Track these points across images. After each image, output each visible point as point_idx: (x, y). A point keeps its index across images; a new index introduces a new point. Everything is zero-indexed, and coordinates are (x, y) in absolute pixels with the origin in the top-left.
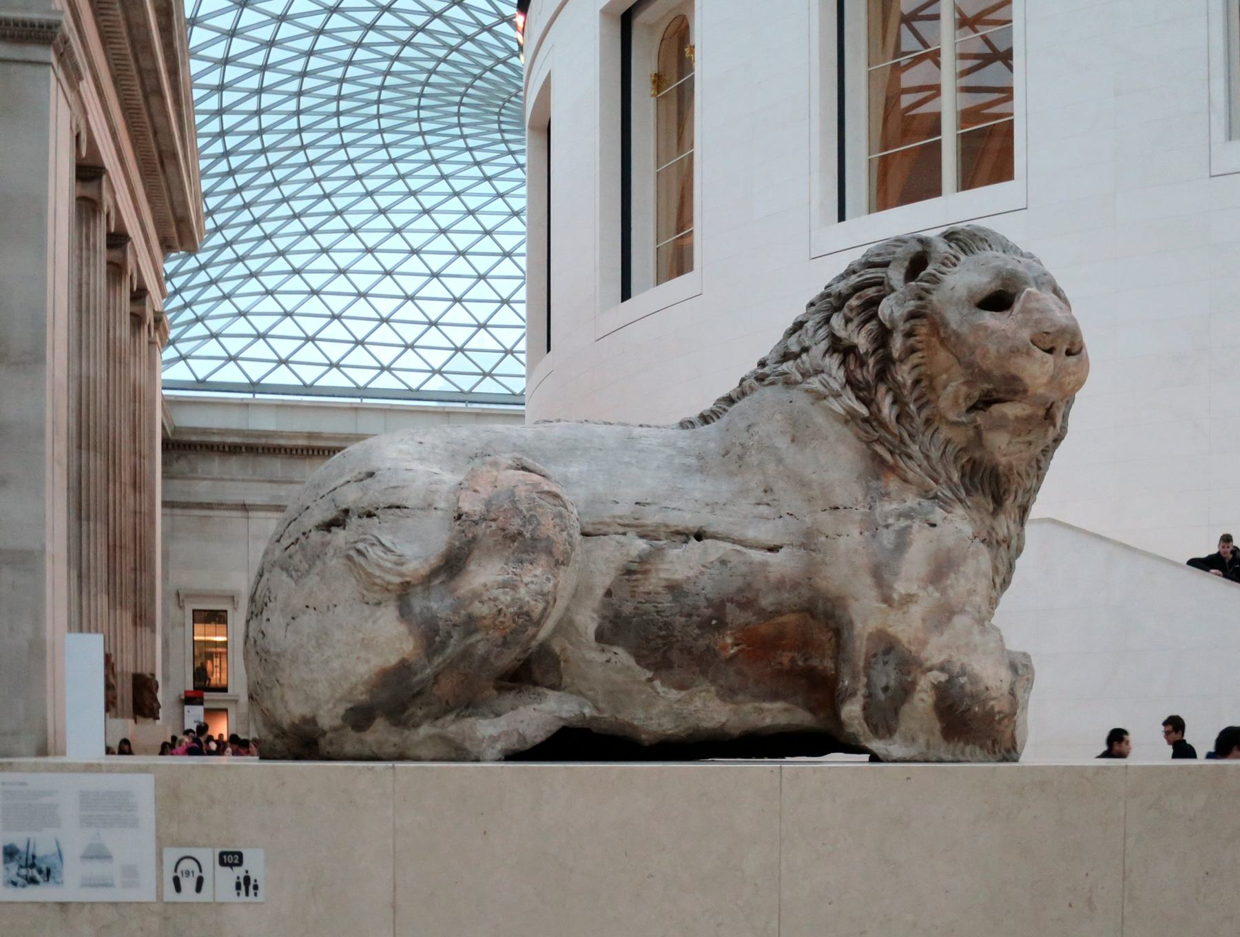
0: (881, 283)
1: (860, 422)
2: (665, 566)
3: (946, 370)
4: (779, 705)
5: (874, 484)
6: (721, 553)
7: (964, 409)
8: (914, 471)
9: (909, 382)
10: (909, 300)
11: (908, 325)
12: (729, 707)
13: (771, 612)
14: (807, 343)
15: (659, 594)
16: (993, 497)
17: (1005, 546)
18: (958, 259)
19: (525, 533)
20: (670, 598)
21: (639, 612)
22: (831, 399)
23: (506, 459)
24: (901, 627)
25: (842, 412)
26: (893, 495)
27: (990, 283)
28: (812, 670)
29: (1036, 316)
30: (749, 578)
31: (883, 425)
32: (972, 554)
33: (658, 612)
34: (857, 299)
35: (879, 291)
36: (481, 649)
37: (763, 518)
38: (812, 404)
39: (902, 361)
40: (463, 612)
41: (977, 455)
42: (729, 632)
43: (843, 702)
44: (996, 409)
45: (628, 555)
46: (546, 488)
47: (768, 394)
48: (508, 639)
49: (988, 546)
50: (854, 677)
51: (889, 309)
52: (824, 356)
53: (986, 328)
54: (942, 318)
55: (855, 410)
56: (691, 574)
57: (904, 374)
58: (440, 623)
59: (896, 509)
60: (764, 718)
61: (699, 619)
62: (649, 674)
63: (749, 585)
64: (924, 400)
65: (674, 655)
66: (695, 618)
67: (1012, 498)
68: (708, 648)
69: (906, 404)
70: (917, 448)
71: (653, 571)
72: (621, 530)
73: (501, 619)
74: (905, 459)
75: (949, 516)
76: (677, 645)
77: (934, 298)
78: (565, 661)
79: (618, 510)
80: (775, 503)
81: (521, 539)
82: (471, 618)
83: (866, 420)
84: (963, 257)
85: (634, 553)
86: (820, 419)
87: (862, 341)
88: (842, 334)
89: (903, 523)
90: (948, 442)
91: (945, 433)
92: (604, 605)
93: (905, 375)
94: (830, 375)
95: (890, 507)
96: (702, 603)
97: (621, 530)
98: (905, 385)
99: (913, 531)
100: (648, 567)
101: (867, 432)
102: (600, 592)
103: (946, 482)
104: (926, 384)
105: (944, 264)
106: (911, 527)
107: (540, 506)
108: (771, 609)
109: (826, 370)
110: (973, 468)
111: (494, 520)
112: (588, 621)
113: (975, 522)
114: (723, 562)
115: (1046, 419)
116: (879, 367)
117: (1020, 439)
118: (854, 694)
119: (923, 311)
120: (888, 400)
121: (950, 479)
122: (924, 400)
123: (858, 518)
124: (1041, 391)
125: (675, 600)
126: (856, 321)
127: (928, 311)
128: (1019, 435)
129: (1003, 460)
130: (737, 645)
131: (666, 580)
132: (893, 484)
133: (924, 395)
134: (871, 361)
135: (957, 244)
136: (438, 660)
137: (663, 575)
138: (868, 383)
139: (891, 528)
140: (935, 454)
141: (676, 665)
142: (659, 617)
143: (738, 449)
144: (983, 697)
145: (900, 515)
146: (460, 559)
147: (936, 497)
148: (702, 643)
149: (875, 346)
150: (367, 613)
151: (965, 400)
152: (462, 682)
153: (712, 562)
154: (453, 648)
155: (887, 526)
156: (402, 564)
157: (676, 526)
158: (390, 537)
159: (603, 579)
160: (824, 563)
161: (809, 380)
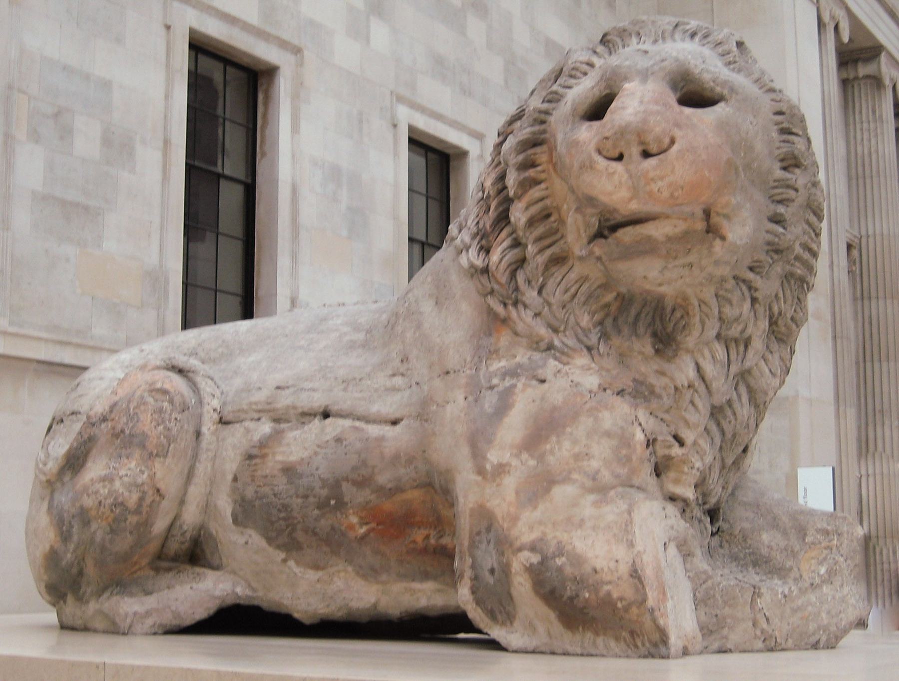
2: (281, 449)
4: (429, 586)
6: (339, 430)
10: (525, 128)
11: (521, 157)
13: (390, 489)
15: (275, 476)
16: (655, 335)
19: (126, 430)
20: (284, 480)
21: (259, 495)
27: (593, 88)
32: (588, 411)
33: (275, 495)
37: (395, 389)
39: (519, 197)
40: (77, 505)
41: (623, 290)
42: (351, 511)
44: (626, 235)
45: (251, 440)
46: (159, 385)
49: (635, 397)
56: (305, 454)
57: (519, 215)
58: (65, 515)
59: (502, 367)
61: (316, 500)
62: (283, 555)
65: (300, 536)
66: (311, 499)
68: (333, 528)
70: (535, 293)
71: (270, 455)
72: (256, 416)
75: (567, 368)
76: (299, 527)
77: (552, 119)
78: (221, 543)
80: (409, 372)
82: (82, 508)
83: (486, 270)
85: (256, 437)
86: (454, 277)
89: (508, 382)
90: (583, 279)
92: (234, 490)
95: (499, 365)
96: (317, 484)
99: (517, 390)
100: (266, 451)
102: (230, 477)
106: (514, 386)
107: (145, 404)
108: (389, 486)
112: (225, 505)
113: (608, 370)
114: (338, 440)
115: (708, 232)
116: (501, 209)
117: (677, 262)
119: (543, 136)
120: (506, 244)
121: (578, 324)
122: (558, 236)
123: (463, 381)
125: (290, 482)
127: (547, 135)
128: (676, 258)
130: (367, 524)
131: (282, 462)
132: (504, 339)
137: (279, 458)
139: (496, 389)
141: (305, 546)
142: (277, 500)
144: (591, 581)
145: (507, 373)
146: (78, 458)
147: (550, 347)
148: (324, 524)
149: (500, 186)
153: (328, 441)
155: (491, 388)
157: (302, 407)
159: (231, 463)
160: (434, 434)
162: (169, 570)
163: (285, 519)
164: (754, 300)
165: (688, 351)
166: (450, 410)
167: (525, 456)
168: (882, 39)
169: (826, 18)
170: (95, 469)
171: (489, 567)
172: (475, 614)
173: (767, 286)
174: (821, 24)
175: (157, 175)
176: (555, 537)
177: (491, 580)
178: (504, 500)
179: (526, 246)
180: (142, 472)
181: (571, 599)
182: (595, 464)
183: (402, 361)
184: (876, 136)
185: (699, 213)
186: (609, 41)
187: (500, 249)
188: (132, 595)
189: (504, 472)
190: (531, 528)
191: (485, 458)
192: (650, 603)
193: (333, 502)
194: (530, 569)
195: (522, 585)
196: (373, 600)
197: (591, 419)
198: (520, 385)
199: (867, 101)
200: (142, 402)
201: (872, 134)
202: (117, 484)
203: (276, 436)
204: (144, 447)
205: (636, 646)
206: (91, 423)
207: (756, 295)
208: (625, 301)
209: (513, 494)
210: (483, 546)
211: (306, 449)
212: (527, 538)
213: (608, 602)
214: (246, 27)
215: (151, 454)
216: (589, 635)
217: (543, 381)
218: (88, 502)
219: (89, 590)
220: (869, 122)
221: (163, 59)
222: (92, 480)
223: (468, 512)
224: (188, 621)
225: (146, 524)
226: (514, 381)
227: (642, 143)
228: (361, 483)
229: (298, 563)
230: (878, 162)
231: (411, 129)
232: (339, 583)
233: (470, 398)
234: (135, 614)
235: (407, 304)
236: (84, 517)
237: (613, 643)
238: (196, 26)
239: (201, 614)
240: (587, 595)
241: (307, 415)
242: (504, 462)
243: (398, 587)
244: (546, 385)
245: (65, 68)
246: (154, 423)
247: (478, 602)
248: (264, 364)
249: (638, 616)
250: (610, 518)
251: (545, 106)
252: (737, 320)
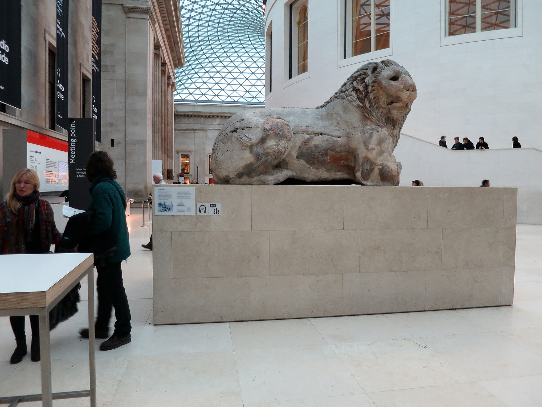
0: (366, 74)
1: (360, 107)
3: (382, 95)
5: (364, 122)
6: (327, 138)
7: (386, 105)
8: (374, 119)
9: (373, 98)
11: (372, 84)
12: (328, 174)
14: (347, 89)
17: (396, 137)
18: (385, 68)
22: (353, 102)
23: (275, 116)
24: (371, 155)
25: (356, 105)
28: (349, 165)
29: (405, 82)
30: (334, 144)
31: (366, 108)
34: (360, 78)
35: (365, 76)
36: (269, 160)
38: (349, 103)
39: (371, 93)
41: (389, 115)
43: (356, 172)
44: (394, 104)
45: (304, 139)
46: (285, 123)
47: (338, 101)
48: (276, 158)
50: (359, 167)
51: (367, 80)
52: (352, 92)
53: (392, 85)
54: (381, 82)
55: (358, 104)
57: (371, 96)
60: (336, 176)
62: (309, 166)
63: (333, 146)
64: (376, 102)
65: (315, 161)
66: (320, 153)
67: (397, 126)
68: (324, 160)
69: (372, 103)
72: (303, 133)
73: (275, 153)
74: (372, 116)
75: (382, 130)
77: (379, 77)
79: (302, 128)
81: (279, 135)
82: (267, 152)
83: (362, 107)
84: (386, 67)
85: (306, 138)
86: (351, 107)
87: (361, 88)
88: (356, 86)
89: (371, 131)
90: (382, 112)
91: (381, 110)
92: (299, 150)
93: (372, 96)
94: (353, 96)
97: (303, 133)
98: (372, 99)
100: (309, 141)
101: (362, 110)
102: (298, 147)
103: (381, 122)
104: (377, 98)
105: (381, 69)
109: (352, 95)
110: (388, 119)
111: (273, 130)
112: (295, 154)
114: (327, 140)
118: (359, 171)
120: (367, 102)
121: (383, 121)
122: (376, 102)
124: (405, 100)
125: (316, 149)
126: (360, 83)
127: (377, 81)
129: (395, 117)
132: (369, 122)
133: (376, 101)
134: (363, 93)
135: (384, 64)
136: (259, 162)
137: (313, 143)
138: (363, 98)
140: (379, 115)
143: (331, 114)
145: (370, 130)
147: (379, 125)
149: (364, 89)
150: (242, 152)
151: (386, 102)
152: (265, 167)
154: (263, 160)
155: (367, 132)
156: (251, 140)
158: (248, 135)
159: (298, 144)
160: (352, 141)
161: (348, 98)
162: (276, 169)
163: (313, 158)
165: (395, 129)
167: (378, 147)
168: (161, 46)
170: (271, 143)
171: (366, 169)
176: (385, 163)
177: (366, 171)
178: (373, 155)
180: (286, 144)
183: (337, 124)
186: (385, 63)
188: (270, 175)
190: (380, 161)
194: (380, 169)
196: (327, 176)
204: (287, 138)
208: (388, 118)
209: (375, 154)
210: (365, 164)
211: (319, 142)
212: (380, 163)
213: (393, 176)
215: (288, 140)
217: (379, 132)
218: (270, 151)
219: (254, 174)
222: (271, 145)
223: (362, 157)
226: (373, 131)
227: (413, 89)
228: (332, 150)
229: (312, 168)
232: (321, 172)
233: (362, 134)
235: (335, 111)
236: (267, 154)
240: (389, 174)
241: (318, 134)
242: (373, 147)
243: (333, 173)
246: (288, 132)
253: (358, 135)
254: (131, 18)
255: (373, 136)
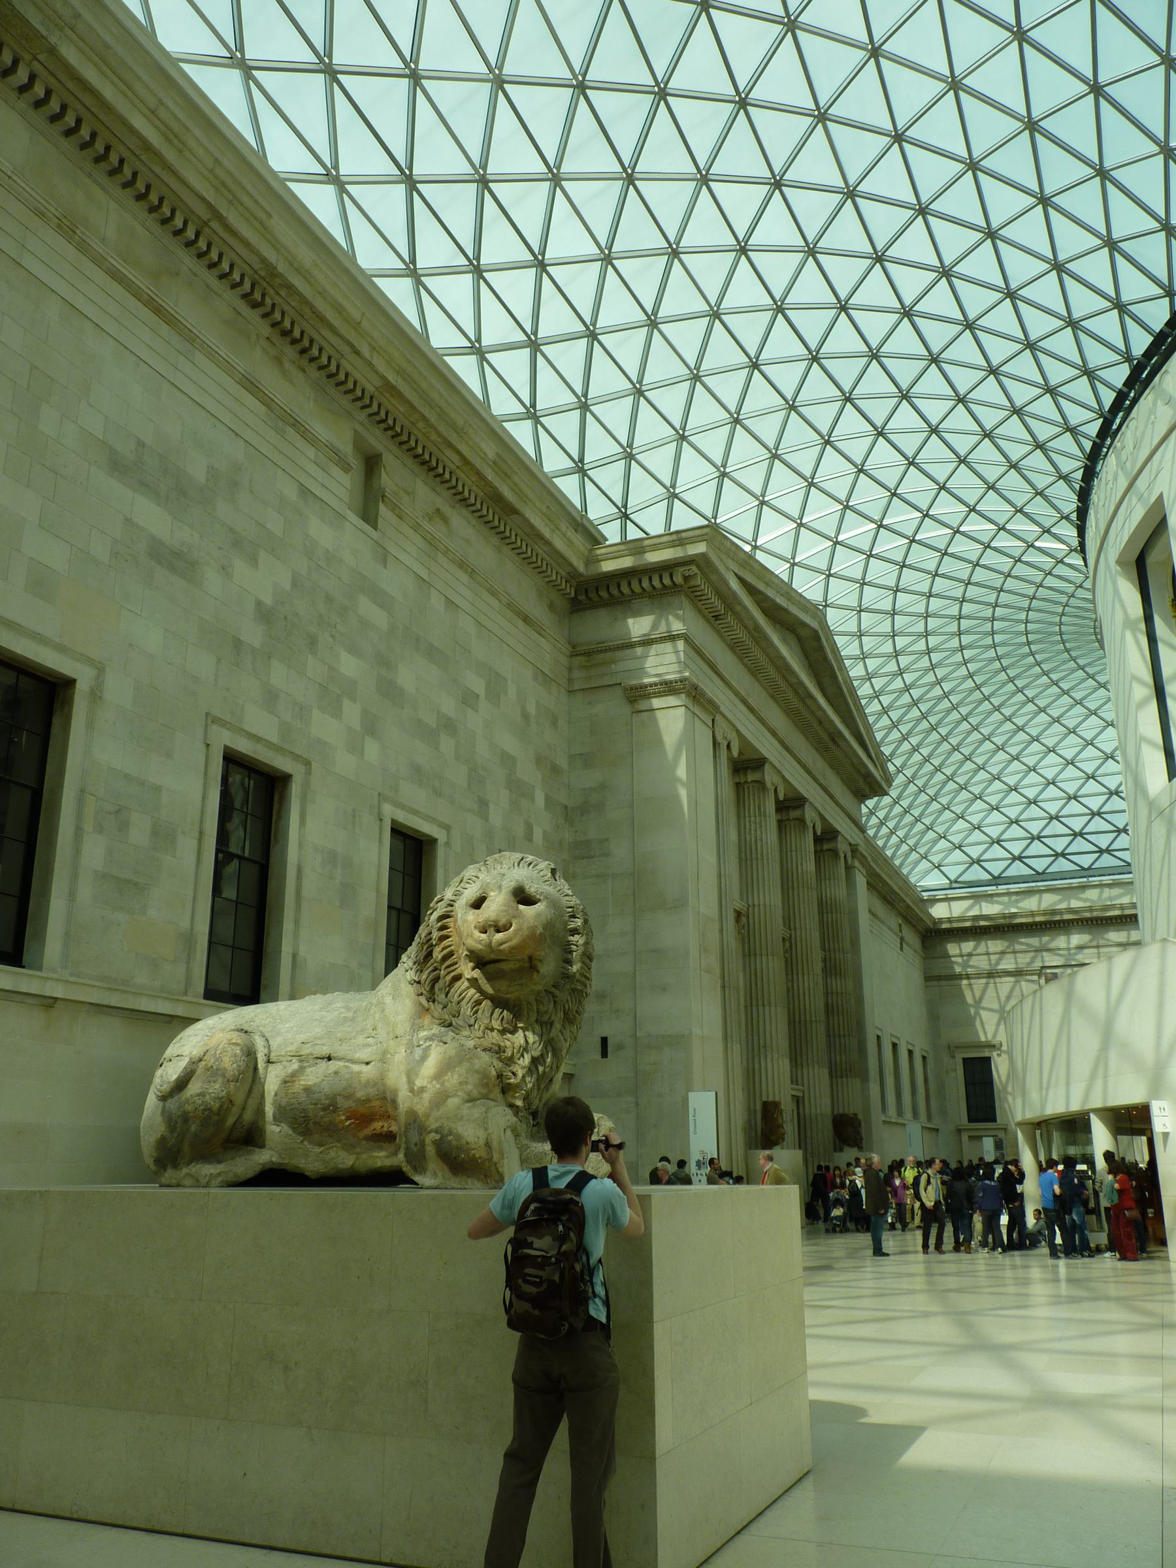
26: (425, 1027)
33: (299, 1104)
37: (369, 1045)
40: (182, 1110)
56: (318, 1080)
62: (302, 1138)
66: (319, 1106)
72: (290, 1058)
76: (311, 1122)
77: (456, 905)
83: (419, 982)
85: (290, 1070)
95: (423, 1034)
96: (323, 1097)
97: (290, 1058)
100: (295, 1079)
102: (273, 1094)
106: (431, 1045)
114: (336, 1073)
122: (457, 966)
123: (405, 1042)
137: (302, 1083)
147: (450, 1025)
155: (419, 1046)
160: (388, 1070)
164: (555, 1002)
166: (397, 1058)
167: (434, 1082)
169: (719, 738)
170: (193, 1088)
172: (407, 1169)
173: (562, 996)
174: (715, 743)
175: (193, 859)
177: (415, 1149)
179: (440, 970)
180: (223, 1091)
181: (455, 1157)
182: (469, 1087)
184: (761, 826)
185: (526, 959)
187: (427, 972)
188: (210, 1163)
189: (423, 1091)
190: (436, 1121)
191: (414, 1083)
192: (495, 1159)
193: (331, 1108)
194: (435, 1143)
195: (430, 1150)
196: (351, 1163)
197: (469, 1064)
198: (434, 1045)
199: (754, 800)
200: (224, 1051)
201: (758, 826)
202: (207, 1097)
203: (302, 1069)
205: (488, 1183)
206: (195, 1063)
207: (556, 999)
211: (318, 1078)
212: (434, 1126)
213: (474, 1160)
214: (269, 745)
216: (464, 1178)
217: (446, 1043)
218: (189, 1108)
220: (755, 817)
221: (203, 770)
224: (243, 1178)
225: (222, 1121)
229: (310, 1143)
230: (762, 847)
231: (393, 822)
232: (332, 1153)
233: (408, 1051)
234: (211, 1174)
236: (186, 1118)
237: (476, 1182)
238: (229, 744)
239: (250, 1174)
244: (447, 1045)
245: (126, 776)
247: (408, 1162)
248: (295, 1029)
249: (489, 1167)
250: (477, 1115)
251: (453, 898)
252: (546, 1012)
253: (400, 1057)
254: (640, 712)
255: (429, 1056)
